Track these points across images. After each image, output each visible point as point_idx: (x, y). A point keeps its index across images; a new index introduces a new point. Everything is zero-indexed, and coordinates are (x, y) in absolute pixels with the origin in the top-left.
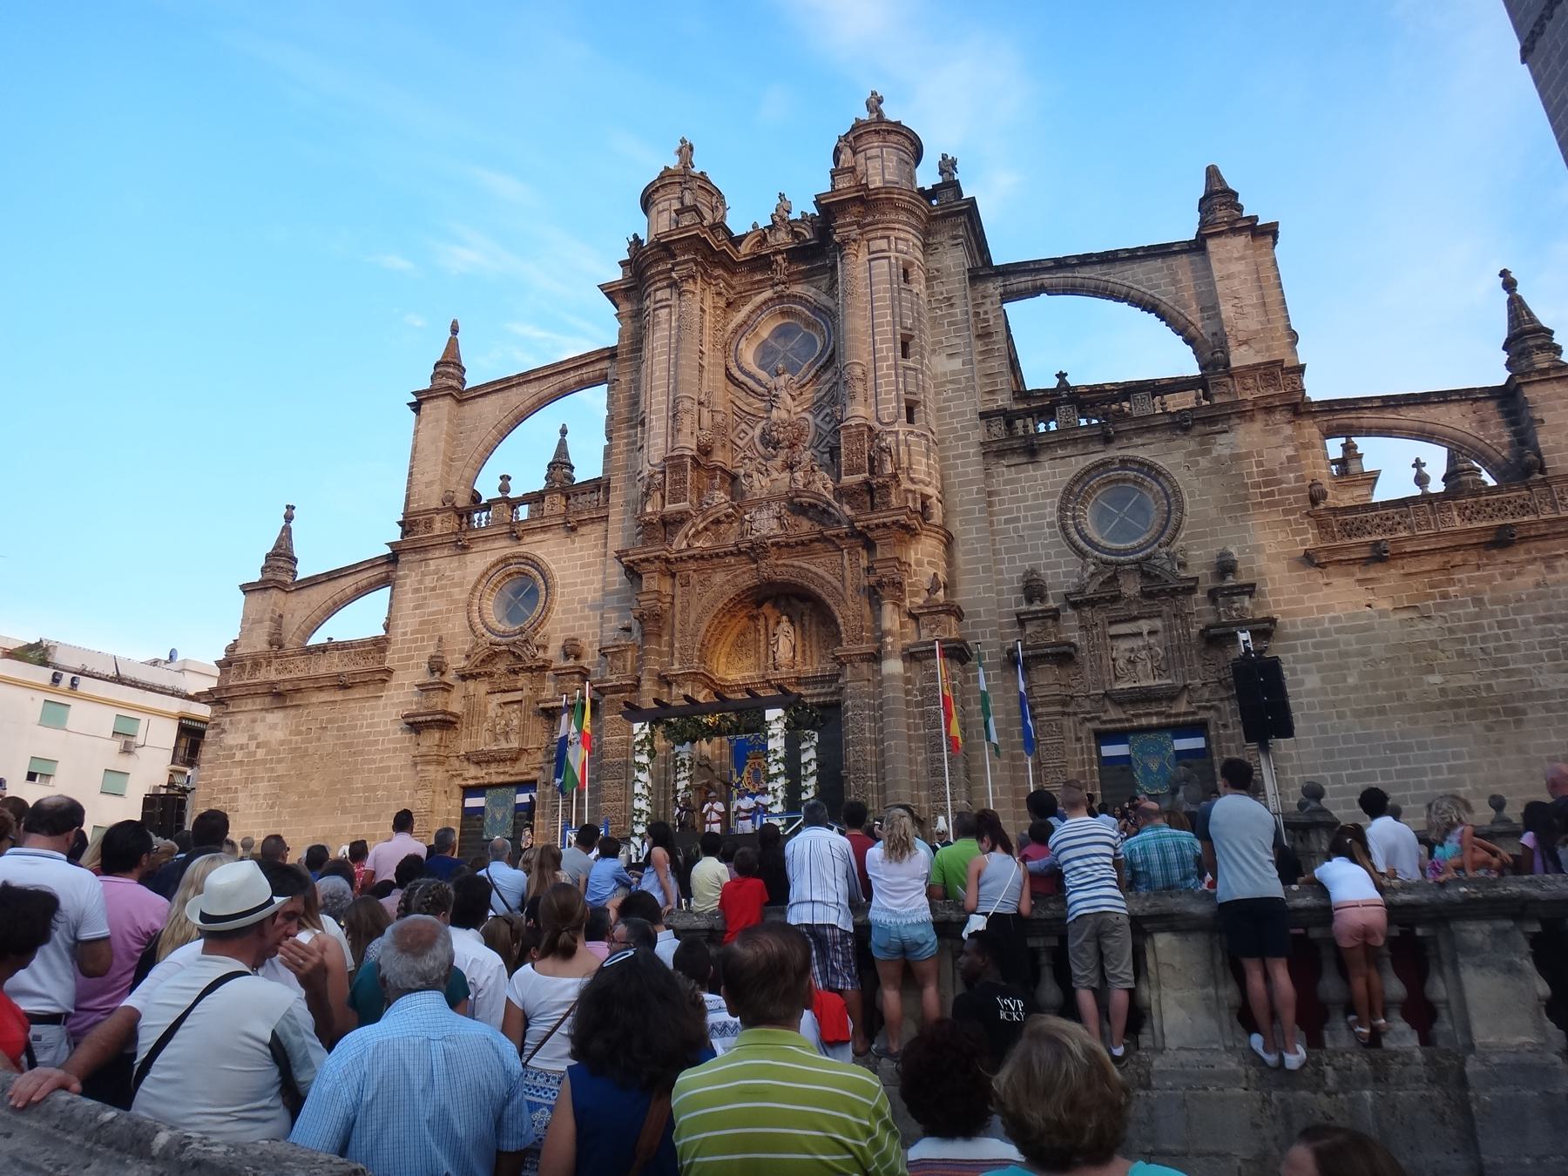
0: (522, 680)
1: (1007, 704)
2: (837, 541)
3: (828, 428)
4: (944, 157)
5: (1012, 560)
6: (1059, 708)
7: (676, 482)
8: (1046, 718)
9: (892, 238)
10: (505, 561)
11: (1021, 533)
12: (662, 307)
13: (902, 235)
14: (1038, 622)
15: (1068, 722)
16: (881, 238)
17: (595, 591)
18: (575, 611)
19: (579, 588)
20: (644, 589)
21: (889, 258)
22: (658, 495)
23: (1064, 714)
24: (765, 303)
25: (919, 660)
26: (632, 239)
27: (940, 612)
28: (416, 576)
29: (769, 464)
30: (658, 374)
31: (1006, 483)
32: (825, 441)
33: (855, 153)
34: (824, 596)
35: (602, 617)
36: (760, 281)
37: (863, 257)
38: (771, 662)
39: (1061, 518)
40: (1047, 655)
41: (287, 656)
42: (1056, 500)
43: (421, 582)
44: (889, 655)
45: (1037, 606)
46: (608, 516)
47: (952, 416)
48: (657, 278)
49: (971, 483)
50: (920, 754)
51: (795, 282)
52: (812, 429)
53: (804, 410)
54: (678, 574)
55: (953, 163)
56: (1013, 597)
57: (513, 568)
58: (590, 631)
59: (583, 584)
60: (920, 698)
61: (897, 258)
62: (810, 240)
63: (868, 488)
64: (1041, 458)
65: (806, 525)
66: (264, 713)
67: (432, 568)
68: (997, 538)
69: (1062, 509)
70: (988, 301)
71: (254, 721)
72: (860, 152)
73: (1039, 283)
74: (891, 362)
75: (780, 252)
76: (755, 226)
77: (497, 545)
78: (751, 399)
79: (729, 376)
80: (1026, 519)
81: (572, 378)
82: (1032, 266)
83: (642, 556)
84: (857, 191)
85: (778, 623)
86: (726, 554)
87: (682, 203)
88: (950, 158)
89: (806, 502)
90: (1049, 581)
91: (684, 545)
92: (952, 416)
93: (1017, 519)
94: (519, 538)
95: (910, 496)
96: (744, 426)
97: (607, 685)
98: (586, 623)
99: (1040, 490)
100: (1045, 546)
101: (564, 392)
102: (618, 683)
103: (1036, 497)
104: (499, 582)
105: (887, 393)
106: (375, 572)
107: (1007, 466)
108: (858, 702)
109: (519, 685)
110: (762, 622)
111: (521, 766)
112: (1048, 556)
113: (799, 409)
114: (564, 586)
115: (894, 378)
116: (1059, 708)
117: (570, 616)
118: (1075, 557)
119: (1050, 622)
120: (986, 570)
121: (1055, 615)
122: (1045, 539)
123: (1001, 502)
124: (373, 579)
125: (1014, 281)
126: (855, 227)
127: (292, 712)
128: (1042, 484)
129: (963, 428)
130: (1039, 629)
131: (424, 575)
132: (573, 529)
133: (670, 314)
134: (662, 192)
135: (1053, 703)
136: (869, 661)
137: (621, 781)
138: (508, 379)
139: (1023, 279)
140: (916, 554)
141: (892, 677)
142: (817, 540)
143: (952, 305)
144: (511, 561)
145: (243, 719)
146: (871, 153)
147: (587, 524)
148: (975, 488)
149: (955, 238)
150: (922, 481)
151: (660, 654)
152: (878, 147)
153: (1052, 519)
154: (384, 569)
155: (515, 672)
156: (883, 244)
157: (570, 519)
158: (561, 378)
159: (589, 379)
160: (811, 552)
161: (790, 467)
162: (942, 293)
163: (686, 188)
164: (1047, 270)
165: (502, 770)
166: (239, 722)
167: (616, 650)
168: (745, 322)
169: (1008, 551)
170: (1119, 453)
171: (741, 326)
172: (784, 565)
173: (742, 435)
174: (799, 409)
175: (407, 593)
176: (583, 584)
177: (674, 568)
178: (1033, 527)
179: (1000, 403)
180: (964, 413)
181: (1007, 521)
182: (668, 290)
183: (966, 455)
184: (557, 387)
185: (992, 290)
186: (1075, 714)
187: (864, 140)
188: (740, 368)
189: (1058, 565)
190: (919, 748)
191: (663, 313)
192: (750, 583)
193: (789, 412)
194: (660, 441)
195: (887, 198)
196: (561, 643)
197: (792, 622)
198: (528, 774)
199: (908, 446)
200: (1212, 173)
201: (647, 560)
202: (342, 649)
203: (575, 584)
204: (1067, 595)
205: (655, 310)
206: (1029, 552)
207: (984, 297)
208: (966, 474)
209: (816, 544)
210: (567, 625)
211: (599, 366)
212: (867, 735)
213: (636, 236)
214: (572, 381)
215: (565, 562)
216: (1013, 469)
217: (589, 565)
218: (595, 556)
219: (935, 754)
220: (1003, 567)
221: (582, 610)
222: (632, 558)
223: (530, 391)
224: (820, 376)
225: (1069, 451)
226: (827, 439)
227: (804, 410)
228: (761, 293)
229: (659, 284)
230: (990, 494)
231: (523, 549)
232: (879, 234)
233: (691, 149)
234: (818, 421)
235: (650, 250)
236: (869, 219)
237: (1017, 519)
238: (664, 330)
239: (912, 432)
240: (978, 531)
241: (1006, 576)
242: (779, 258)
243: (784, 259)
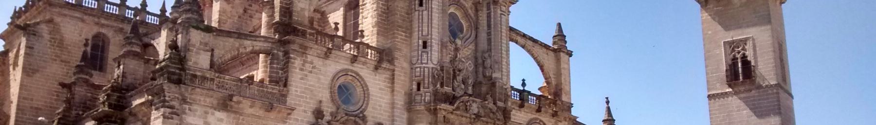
28: (301, 60)
41: (224, 79)
43: (303, 65)
59: (380, 98)
66: (212, 110)
67: (309, 58)
71: (206, 113)
82: (518, 32)
106: (266, 45)
114: (372, 95)
124: (262, 48)
127: (233, 115)
131: (305, 62)
145: (199, 110)
147: (381, 69)
154: (270, 45)
164: (521, 35)
166: (196, 110)
170: (539, 117)
175: (296, 68)
176: (380, 98)
200: (559, 25)
202: (260, 87)
203: (377, 97)
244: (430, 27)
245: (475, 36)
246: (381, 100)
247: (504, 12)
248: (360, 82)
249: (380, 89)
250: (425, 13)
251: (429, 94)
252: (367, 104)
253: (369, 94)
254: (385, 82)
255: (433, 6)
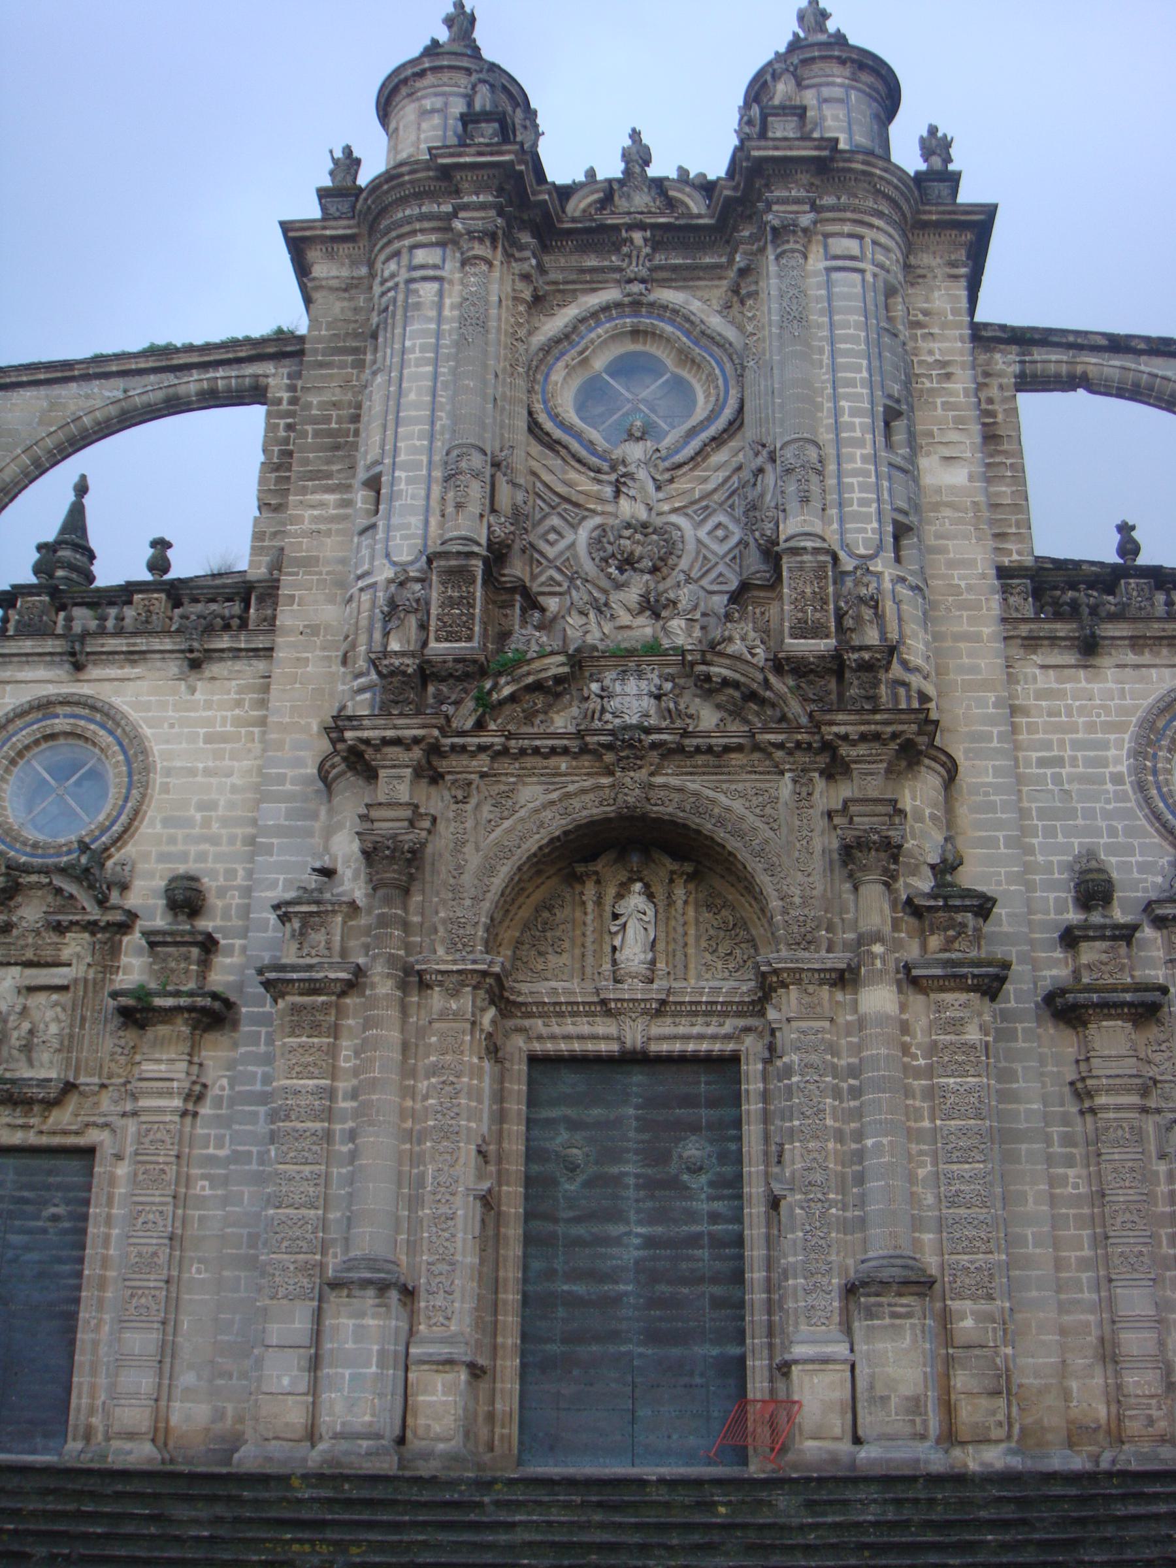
0: (75, 945)
1: (1044, 1085)
2: (779, 754)
3: (721, 549)
4: (933, 130)
5: (1050, 832)
6: (1134, 1099)
7: (450, 602)
8: (1111, 1115)
9: (868, 240)
10: (44, 707)
11: (1066, 787)
12: (425, 279)
13: (883, 239)
14: (1104, 945)
15: (1150, 1125)
16: (851, 236)
17: (234, 789)
18: (188, 822)
19: (199, 779)
20: (382, 798)
21: (862, 271)
22: (412, 621)
23: (1145, 1110)
24: (606, 308)
25: (924, 991)
26: (338, 154)
27: (966, 909)
29: (615, 596)
30: (412, 396)
31: (1041, 695)
32: (713, 575)
33: (799, 84)
34: (743, 855)
35: (251, 841)
36: (593, 270)
37: (816, 262)
38: (607, 967)
39: (1138, 770)
40: (1123, 1004)
42: (1127, 737)
44: (877, 978)
45: (1096, 918)
46: (271, 649)
47: (951, 564)
48: (418, 226)
49: (985, 685)
50: (922, 1164)
51: (664, 283)
52: (691, 546)
53: (675, 510)
54: (448, 777)
55: (946, 144)
56: (1052, 896)
57: (60, 724)
58: (220, 867)
59: (207, 772)
60: (922, 1062)
61: (875, 275)
62: (699, 216)
63: (836, 666)
64: (1105, 661)
65: (708, 717)
68: (1025, 789)
69: (1138, 753)
70: (995, 382)
72: (808, 87)
73: (1079, 369)
74: (869, 450)
75: (642, 227)
76: (591, 173)
77: (28, 674)
78: (572, 475)
79: (534, 428)
80: (1074, 761)
81: (192, 384)
82: (1071, 339)
83: (390, 733)
84: (817, 148)
85: (620, 896)
86: (553, 751)
87: (470, 104)
88: (940, 134)
89: (719, 675)
90: (1115, 875)
91: (469, 724)
92: (951, 564)
93: (1059, 762)
94: (78, 667)
95: (902, 691)
96: (555, 521)
97: (295, 976)
98: (212, 849)
99: (1099, 715)
100: (1107, 815)
101: (174, 406)
102: (320, 975)
103: (1091, 727)
104: (27, 748)
105: (863, 502)
107: (1043, 667)
108: (814, 1058)
109: (66, 954)
110: (590, 891)
111: (63, 1117)
112: (1113, 832)
113: (666, 507)
114: (168, 772)
115: (873, 479)
116: (1134, 1099)
117: (180, 833)
118: (1157, 840)
119: (1123, 950)
120: (1010, 842)
121: (1126, 934)
122: (1108, 802)
123: (1032, 729)
125: (1037, 357)
126: (807, 207)
128: (1102, 707)
129: (970, 588)
130: (1104, 957)
132: (195, 665)
133: (441, 294)
134: (430, 79)
135: (1128, 1090)
136: (833, 985)
137: (316, 1168)
138: (67, 365)
139: (1054, 357)
140: (914, 799)
141: (882, 1019)
142: (739, 748)
143: (948, 376)
144: (60, 710)
146: (826, 92)
147: (222, 659)
148: (992, 697)
149: (953, 264)
150: (917, 669)
151: (406, 926)
152: (841, 85)
153: (1119, 769)
155: (59, 929)
156: (853, 246)
157: (196, 645)
158: (170, 379)
159: (229, 390)
160: (718, 769)
161: (653, 607)
162: (931, 352)
163: (484, 81)
164: (1095, 349)
165: (20, 1121)
167: (314, 908)
168: (567, 336)
169: (1043, 814)
171: (558, 341)
172: (665, 786)
173: (552, 537)
174: (666, 507)
177: (443, 765)
178: (1082, 779)
179: (1015, 557)
180: (971, 563)
181: (1042, 763)
182: (438, 251)
183: (976, 638)
184: (160, 395)
185: (1000, 366)
186: (1158, 1111)
187: (816, 67)
188: (555, 417)
189: (1129, 850)
190: (921, 1153)
191: (428, 291)
192: (596, 812)
193: (650, 509)
194: (415, 521)
195: (864, 173)
196: (163, 884)
197: (650, 896)
198: (77, 1133)
199: (898, 603)
201: (397, 742)
203: (192, 772)
204: (1149, 907)
205: (410, 281)
206: (1080, 822)
207: (987, 374)
208: (974, 669)
209: (733, 756)
210: (172, 849)
211: (250, 369)
212: (829, 1122)
213: (348, 151)
214: (193, 388)
215: (172, 726)
216: (1051, 672)
217: (224, 738)
218: (238, 722)
219: (955, 1167)
220: (1035, 841)
221: (206, 823)
222: (366, 734)
223: (107, 394)
224: (708, 456)
225: (1146, 658)
226: (721, 568)
227: (675, 510)
228: (594, 290)
229: (420, 238)
230: (1014, 710)
231: (85, 689)
232: (847, 228)
233: (472, 20)
234: (702, 533)
235: (411, 172)
236: (829, 200)
237: (1059, 762)
238: (430, 320)
239: (903, 580)
240: (997, 772)
241: (1040, 858)
242: (638, 237)
243: (645, 240)
244: (391, 425)
245: (736, 406)
246: (214, 780)
247: (853, 258)
248: (111, 733)
249: (209, 739)
250: (379, 379)
251: (367, 695)
252: (136, 812)
253: (147, 769)
254: (239, 704)
255: (408, 343)
